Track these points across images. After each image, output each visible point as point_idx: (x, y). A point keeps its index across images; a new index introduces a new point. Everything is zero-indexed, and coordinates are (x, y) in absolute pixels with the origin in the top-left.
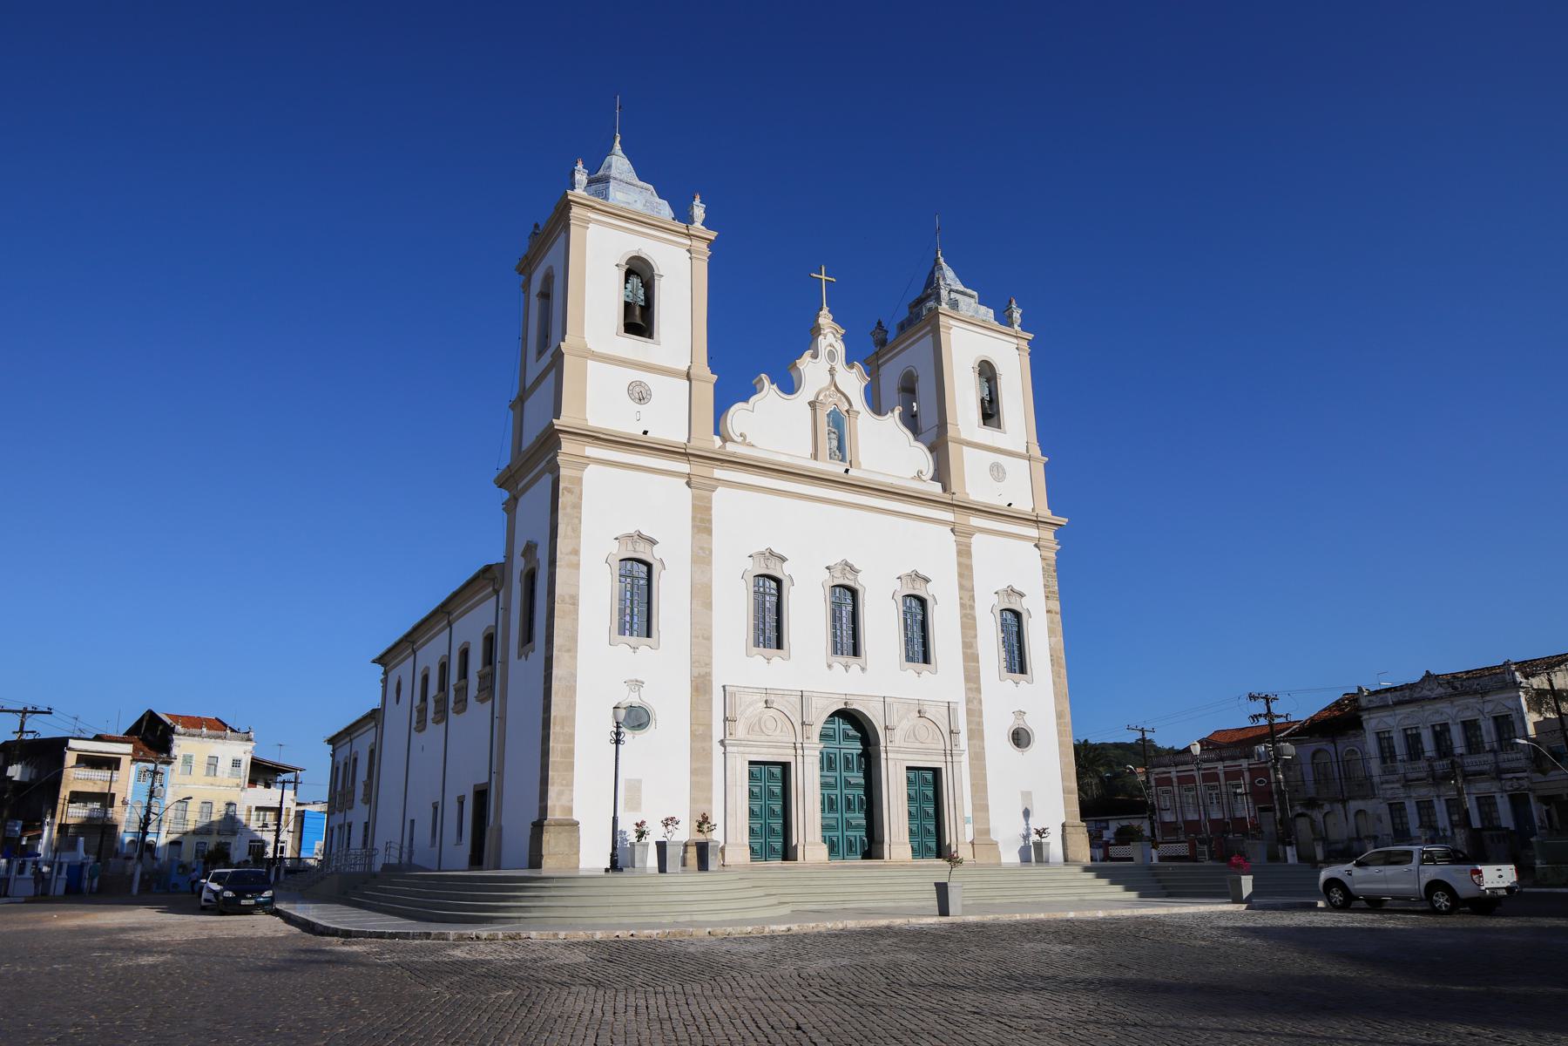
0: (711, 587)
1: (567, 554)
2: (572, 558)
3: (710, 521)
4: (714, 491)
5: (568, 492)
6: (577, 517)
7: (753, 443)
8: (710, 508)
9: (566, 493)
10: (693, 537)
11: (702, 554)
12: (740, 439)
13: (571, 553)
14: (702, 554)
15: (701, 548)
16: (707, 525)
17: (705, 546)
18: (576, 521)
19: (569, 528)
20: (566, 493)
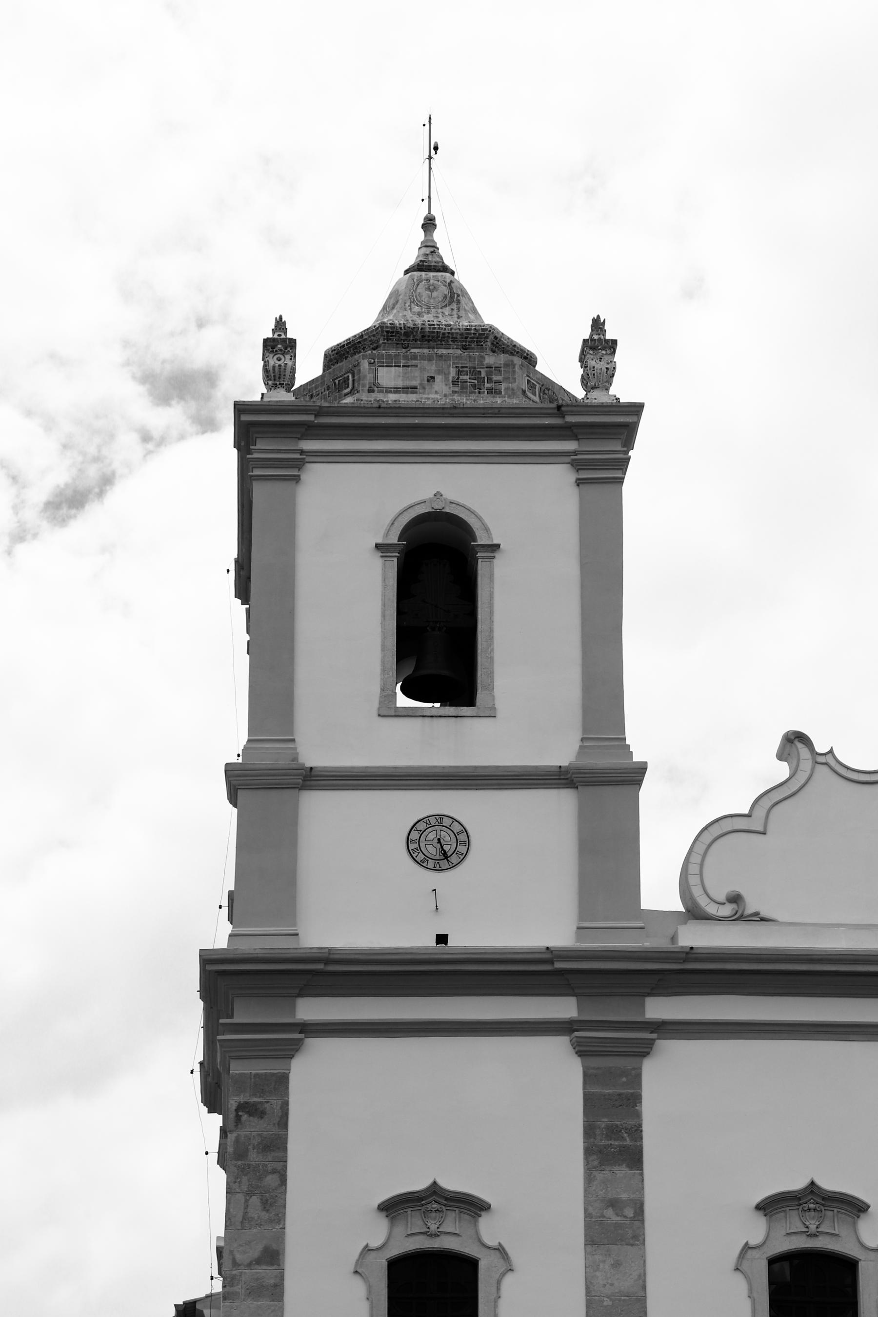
0: (642, 1301)
1: (250, 1265)
2: (266, 1272)
3: (636, 1132)
4: (645, 1056)
5: (250, 1114)
6: (274, 1171)
7: (764, 913)
8: (636, 1099)
9: (245, 1117)
10: (589, 1179)
11: (616, 1219)
12: (727, 910)
13: (258, 1261)
14: (616, 1219)
15: (614, 1204)
16: (628, 1142)
17: (624, 1196)
18: (271, 1180)
19: (255, 1200)
20: (245, 1117)
